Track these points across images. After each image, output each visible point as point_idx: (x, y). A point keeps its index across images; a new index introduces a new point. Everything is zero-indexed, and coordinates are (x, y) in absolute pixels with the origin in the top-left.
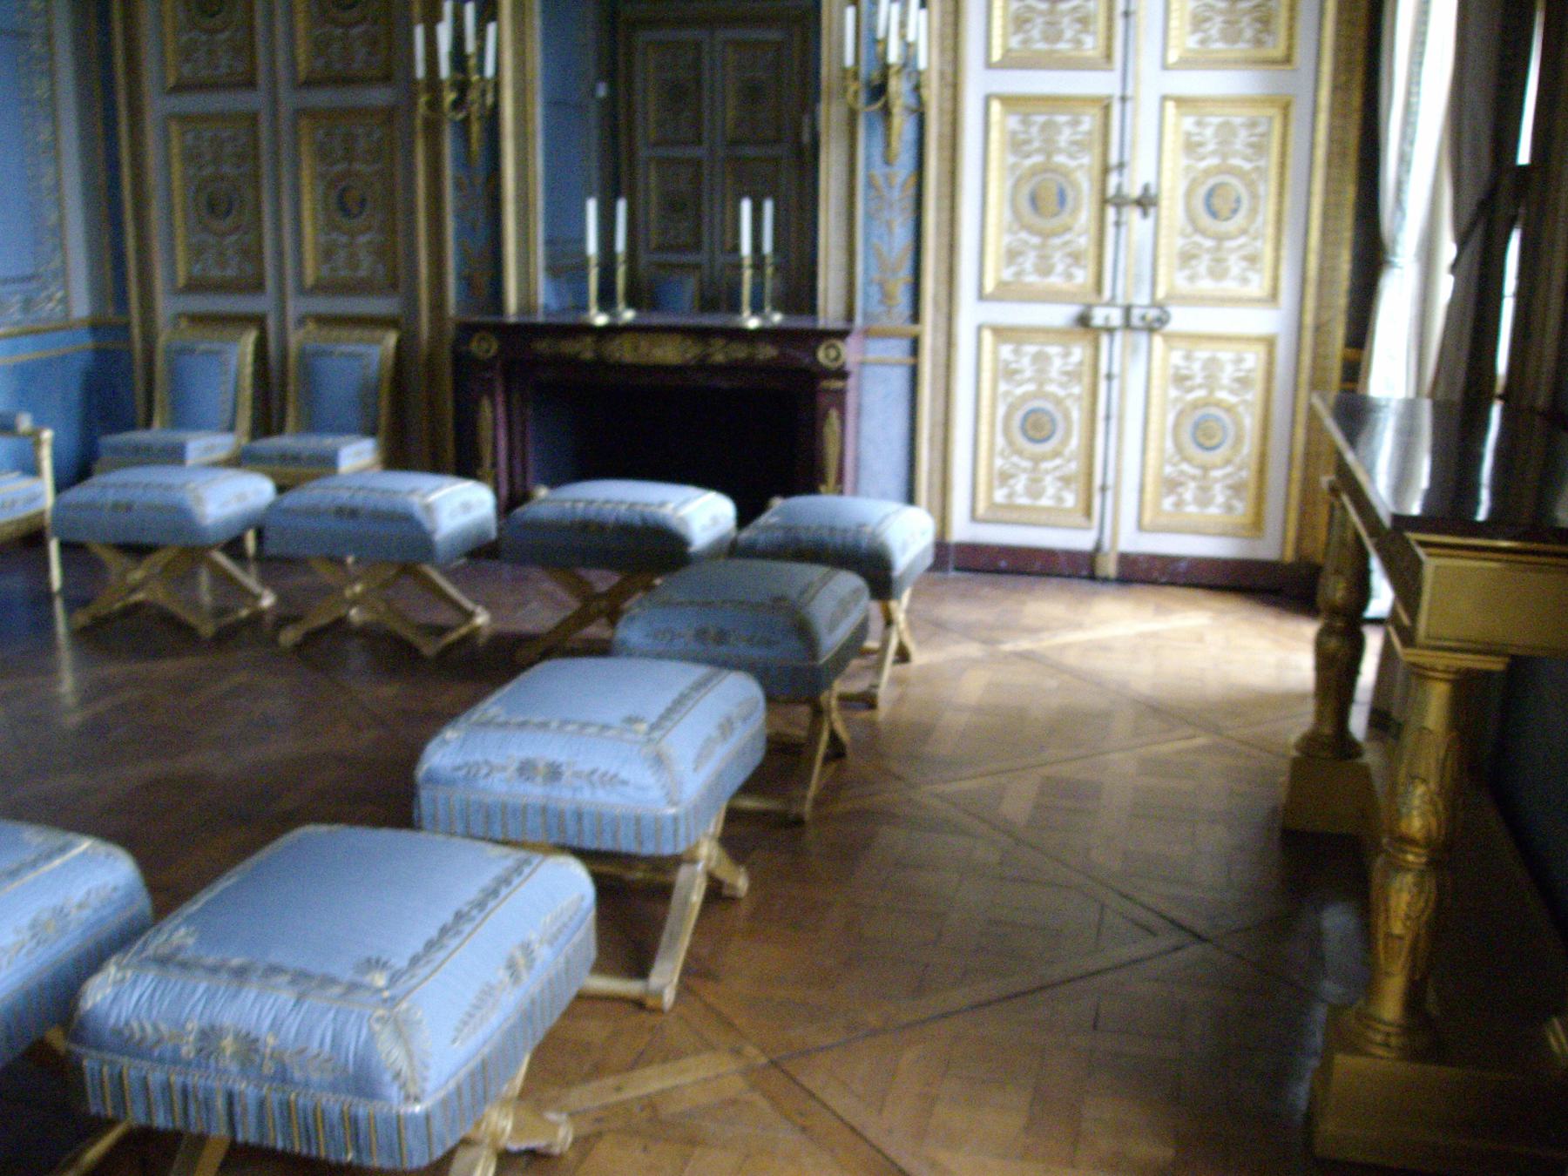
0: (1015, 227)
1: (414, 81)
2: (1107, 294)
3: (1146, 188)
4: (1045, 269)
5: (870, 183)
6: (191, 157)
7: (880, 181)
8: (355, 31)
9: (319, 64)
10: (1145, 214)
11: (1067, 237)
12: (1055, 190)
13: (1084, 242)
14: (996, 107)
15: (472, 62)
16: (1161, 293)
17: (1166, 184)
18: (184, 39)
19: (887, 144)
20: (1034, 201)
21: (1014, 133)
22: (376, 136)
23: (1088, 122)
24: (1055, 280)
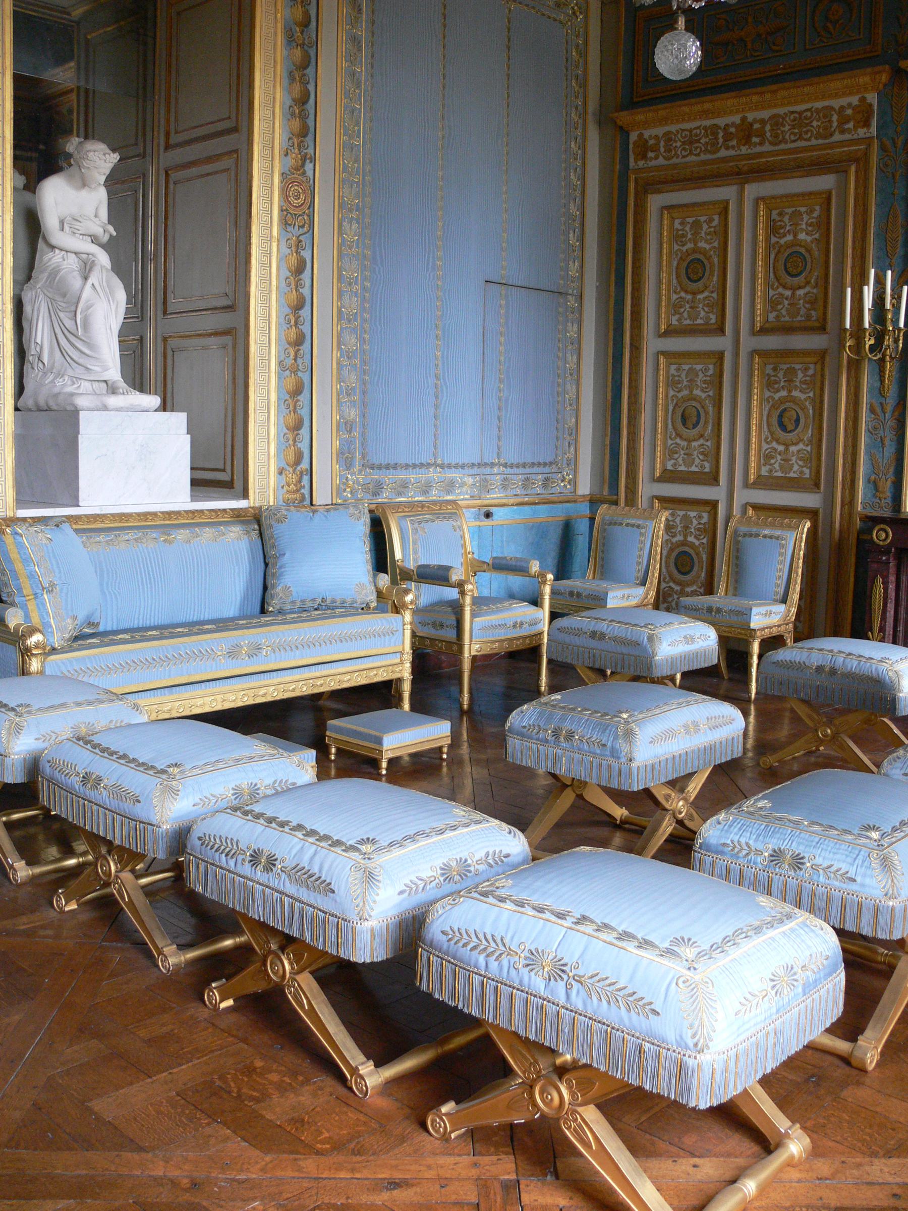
6: (672, 383)
8: (801, 292)
9: (772, 316)
22: (811, 372)
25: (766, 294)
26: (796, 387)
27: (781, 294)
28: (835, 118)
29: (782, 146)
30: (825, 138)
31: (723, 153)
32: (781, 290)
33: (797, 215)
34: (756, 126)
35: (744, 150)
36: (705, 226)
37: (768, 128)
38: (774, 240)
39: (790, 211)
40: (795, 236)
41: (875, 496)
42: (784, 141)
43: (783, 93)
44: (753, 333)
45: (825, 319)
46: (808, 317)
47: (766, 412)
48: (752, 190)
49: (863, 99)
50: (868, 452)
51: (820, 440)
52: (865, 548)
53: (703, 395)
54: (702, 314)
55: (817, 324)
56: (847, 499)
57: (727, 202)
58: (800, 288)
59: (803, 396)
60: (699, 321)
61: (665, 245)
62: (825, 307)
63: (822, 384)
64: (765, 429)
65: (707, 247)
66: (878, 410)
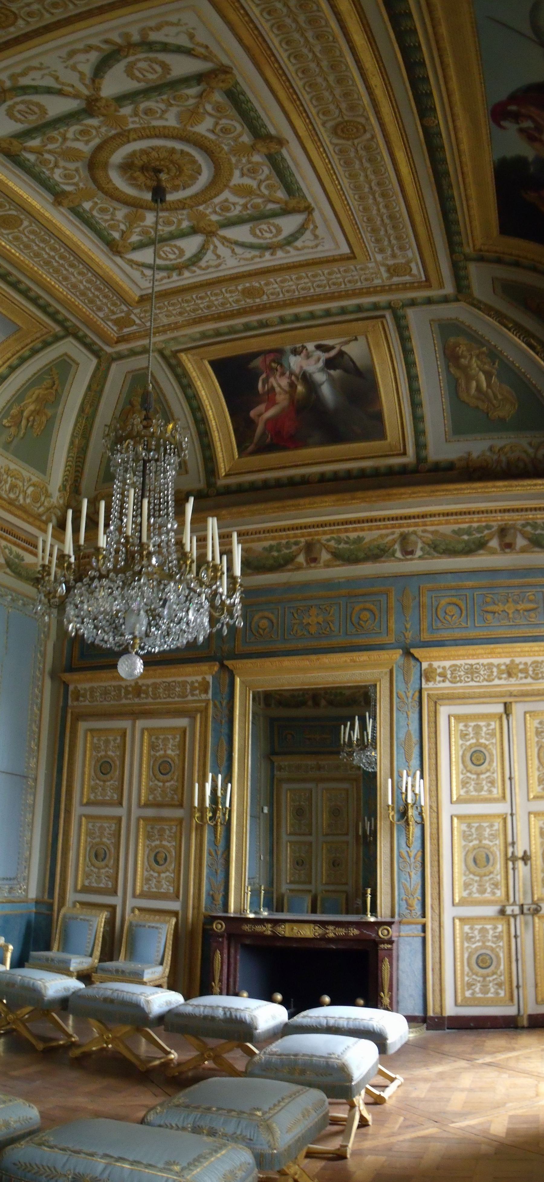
0: (467, 873)
1: (192, 807)
2: (511, 900)
3: (525, 852)
4: (482, 891)
5: (400, 855)
7: (405, 854)
9: (151, 797)
10: (526, 864)
11: (491, 876)
12: (484, 856)
13: (500, 878)
14: (455, 820)
15: (220, 800)
16: (536, 898)
17: (533, 850)
18: (92, 783)
19: (408, 839)
20: (475, 861)
21: (464, 832)
22: (174, 830)
23: (498, 825)
24: (487, 896)
25: (147, 784)
26: (165, 839)
27: (156, 785)
28: (188, 687)
29: (159, 700)
30: (183, 697)
31: (124, 701)
32: (156, 782)
33: (166, 740)
34: (144, 688)
35: (136, 700)
36: (112, 743)
37: (150, 689)
38: (152, 753)
39: (162, 737)
40: (165, 751)
41: (212, 903)
42: (160, 697)
43: (159, 671)
44: (139, 806)
45: (182, 800)
46: (172, 799)
47: (147, 852)
48: (140, 724)
49: (204, 679)
50: (208, 878)
51: (179, 871)
52: (208, 935)
53: (108, 842)
54: (109, 793)
55: (177, 803)
56: (196, 905)
57: (126, 729)
58: (167, 781)
59: (169, 845)
60: (107, 798)
61: (88, 752)
62: (183, 794)
63: (181, 838)
64: (146, 863)
65: (113, 754)
66: (214, 853)
